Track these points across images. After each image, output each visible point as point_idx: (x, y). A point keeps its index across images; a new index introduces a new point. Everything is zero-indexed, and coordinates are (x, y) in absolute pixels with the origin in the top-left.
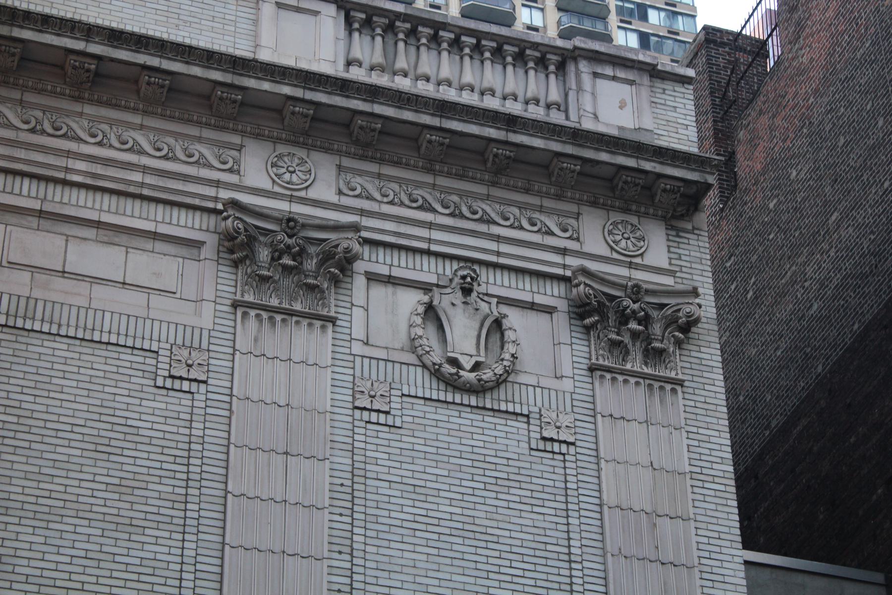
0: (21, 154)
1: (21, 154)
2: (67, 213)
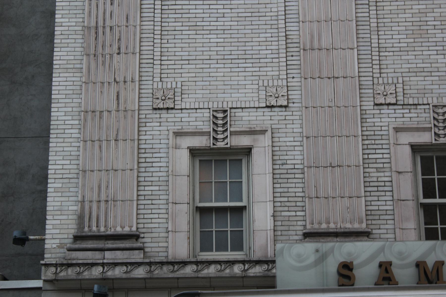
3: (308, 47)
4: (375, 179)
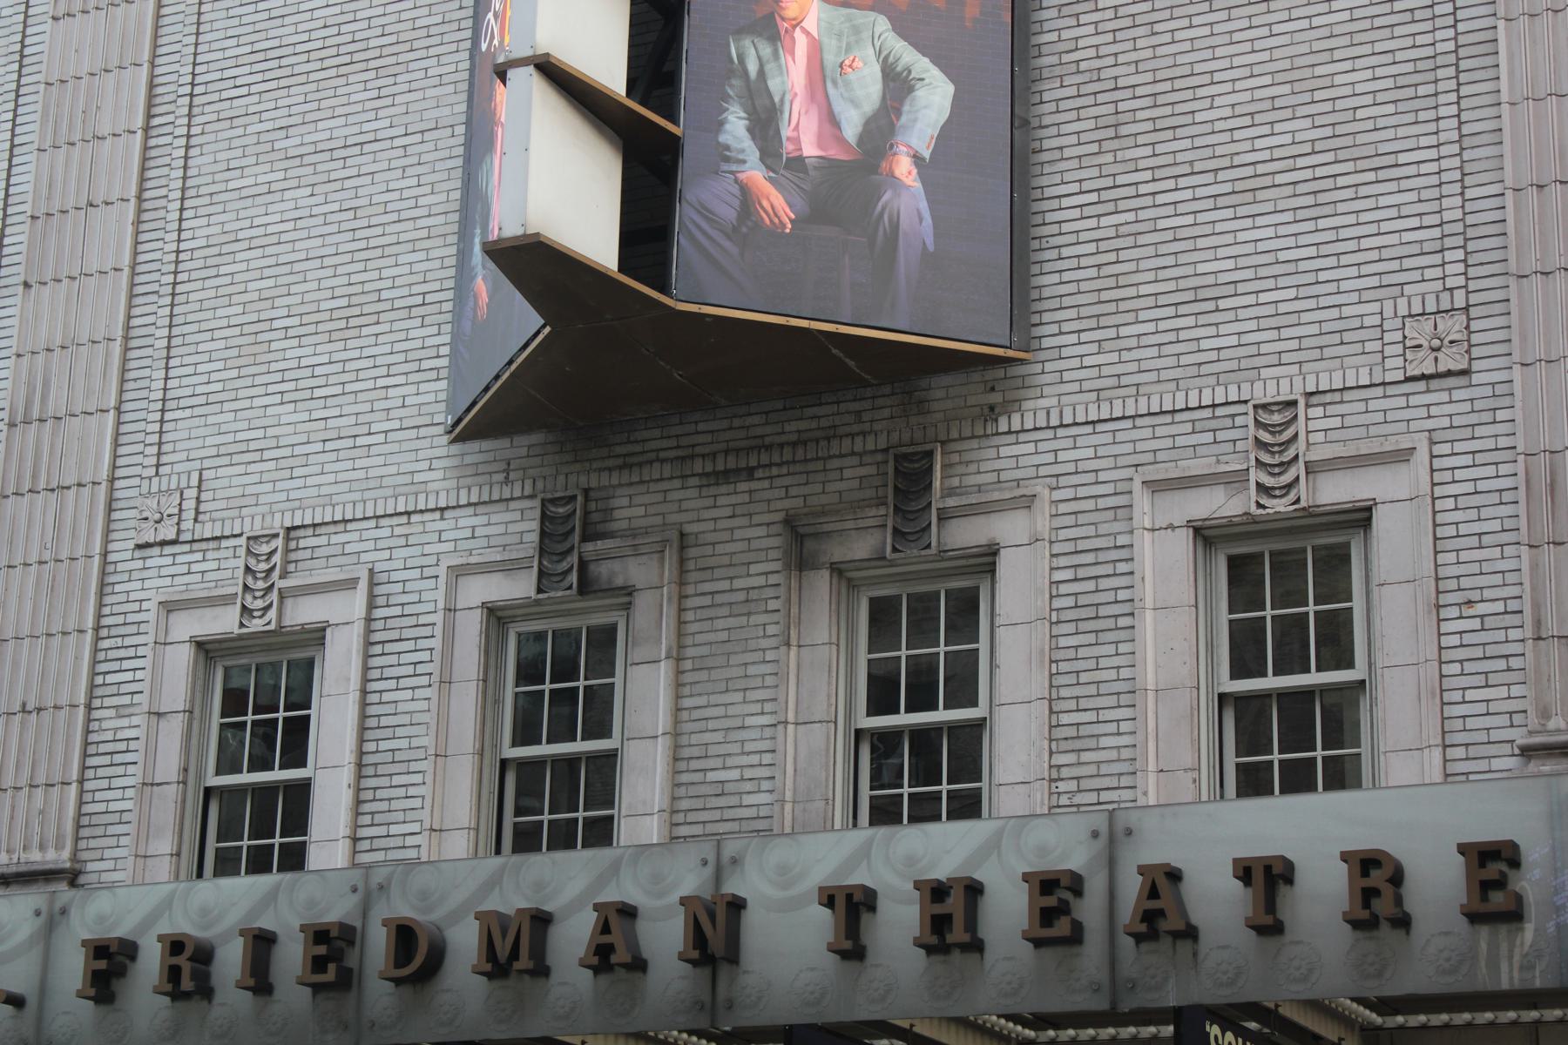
3: (19, 418)
4: (109, 736)
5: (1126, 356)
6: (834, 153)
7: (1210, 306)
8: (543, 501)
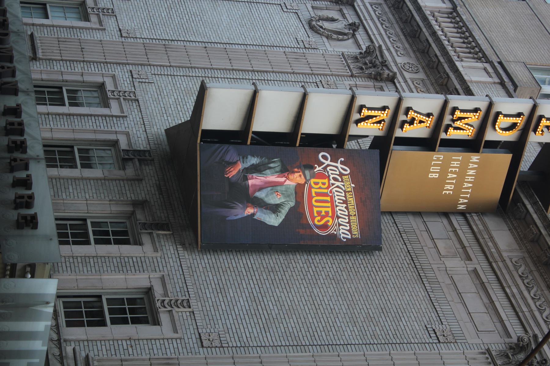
0: (504, 271)
1: (504, 271)
2: (490, 293)
5: (202, 274)
6: (251, 190)
7: (219, 291)
8: (149, 151)
